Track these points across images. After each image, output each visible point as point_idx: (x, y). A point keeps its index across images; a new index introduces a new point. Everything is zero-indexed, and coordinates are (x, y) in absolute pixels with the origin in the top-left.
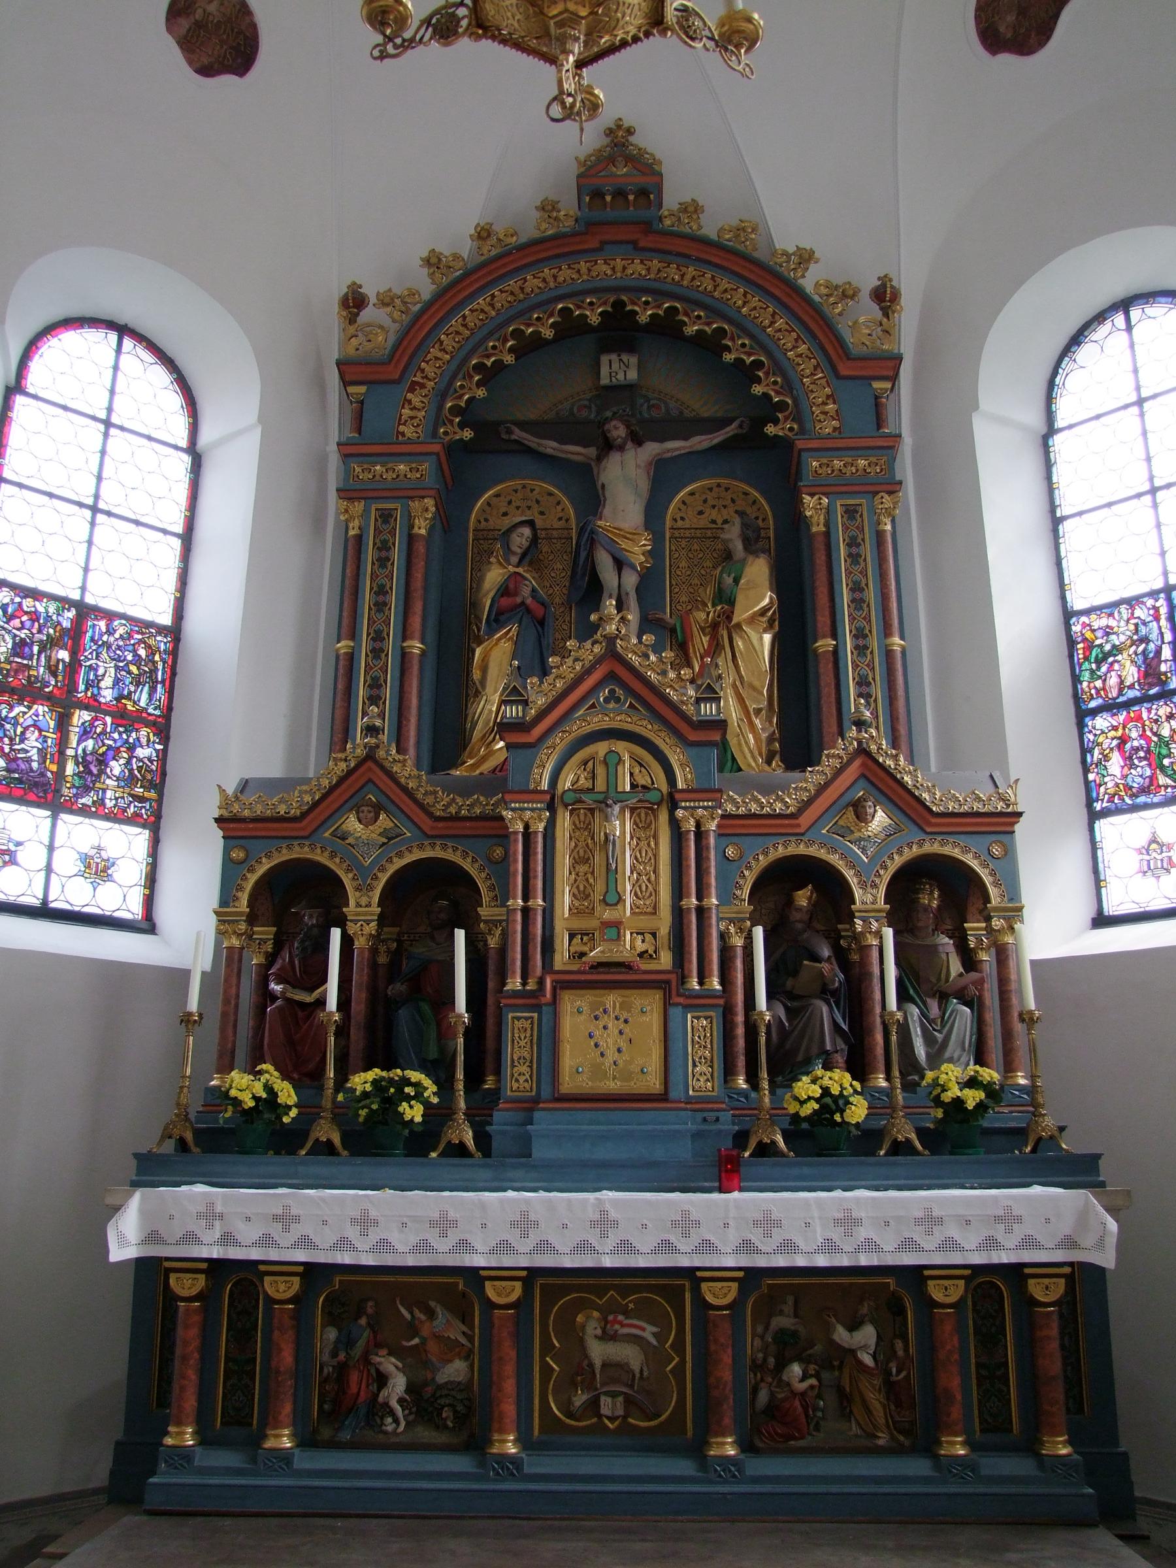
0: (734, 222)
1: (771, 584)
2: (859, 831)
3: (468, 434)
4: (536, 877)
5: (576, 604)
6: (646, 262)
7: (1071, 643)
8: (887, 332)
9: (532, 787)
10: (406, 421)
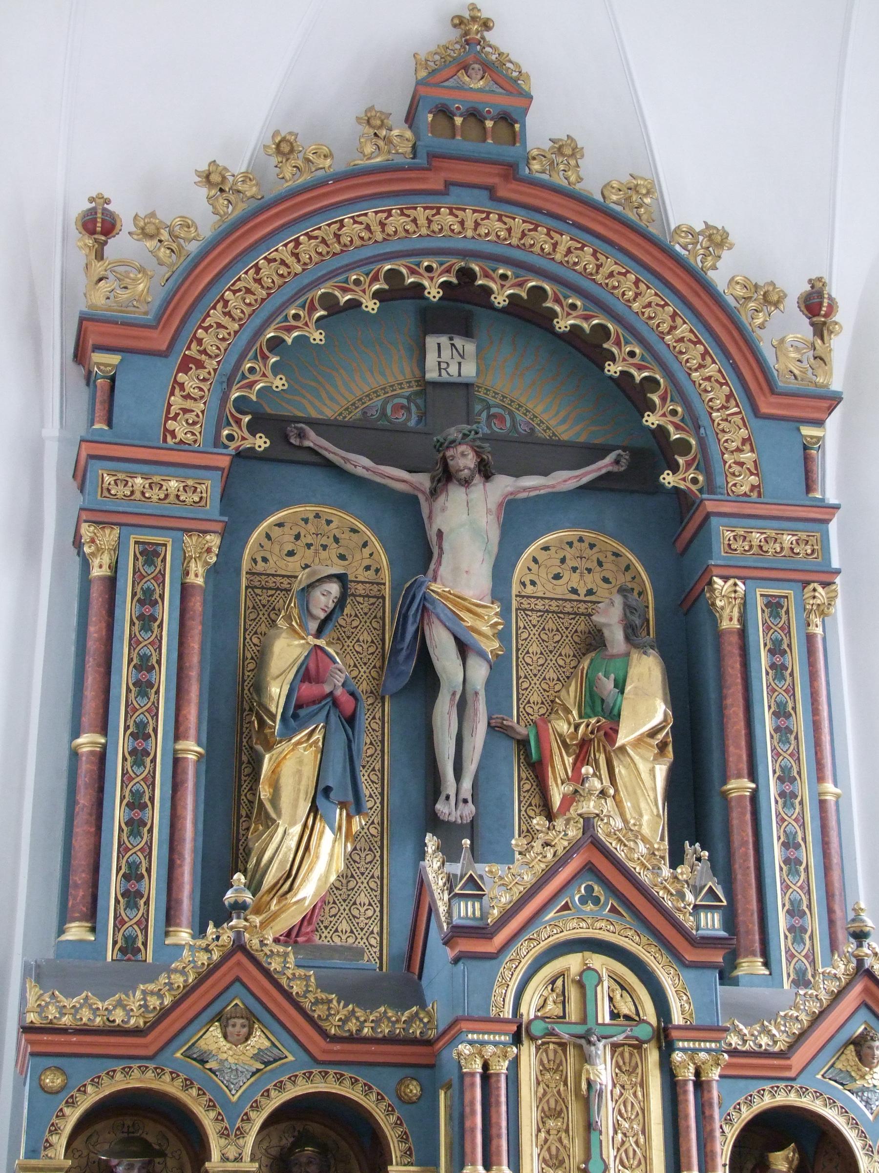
0: (626, 179)
1: (665, 694)
2: (863, 1077)
3: (261, 442)
4: (499, 1136)
5: (391, 696)
6: (505, 219)
8: (821, 359)
9: (493, 1013)
10: (177, 415)
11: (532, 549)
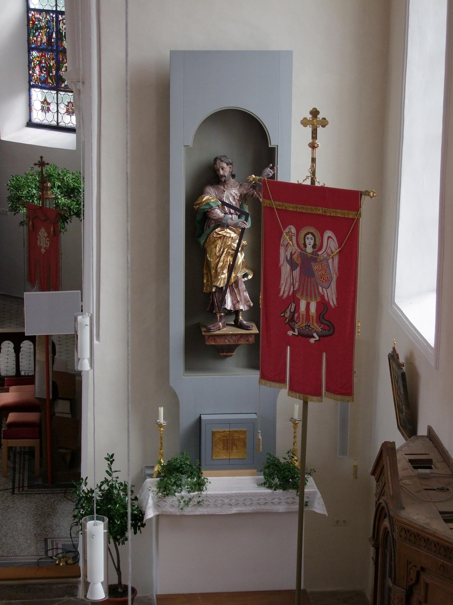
7: (29, 19)
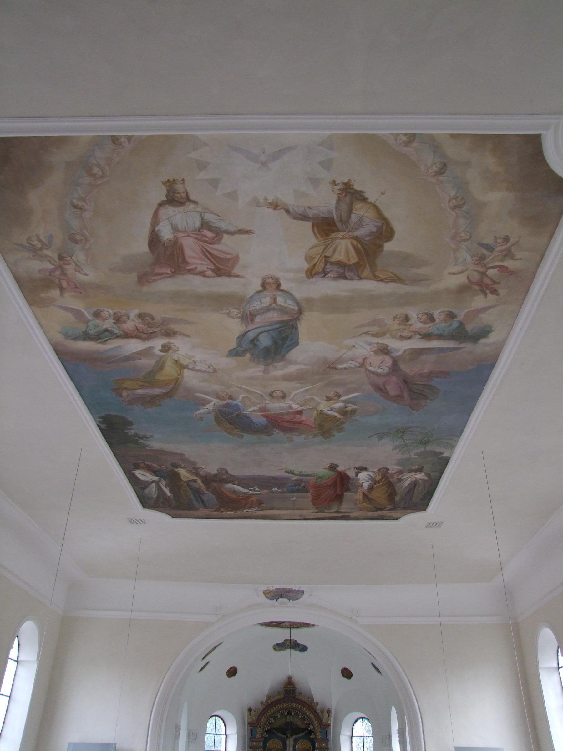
11: (299, 742)
